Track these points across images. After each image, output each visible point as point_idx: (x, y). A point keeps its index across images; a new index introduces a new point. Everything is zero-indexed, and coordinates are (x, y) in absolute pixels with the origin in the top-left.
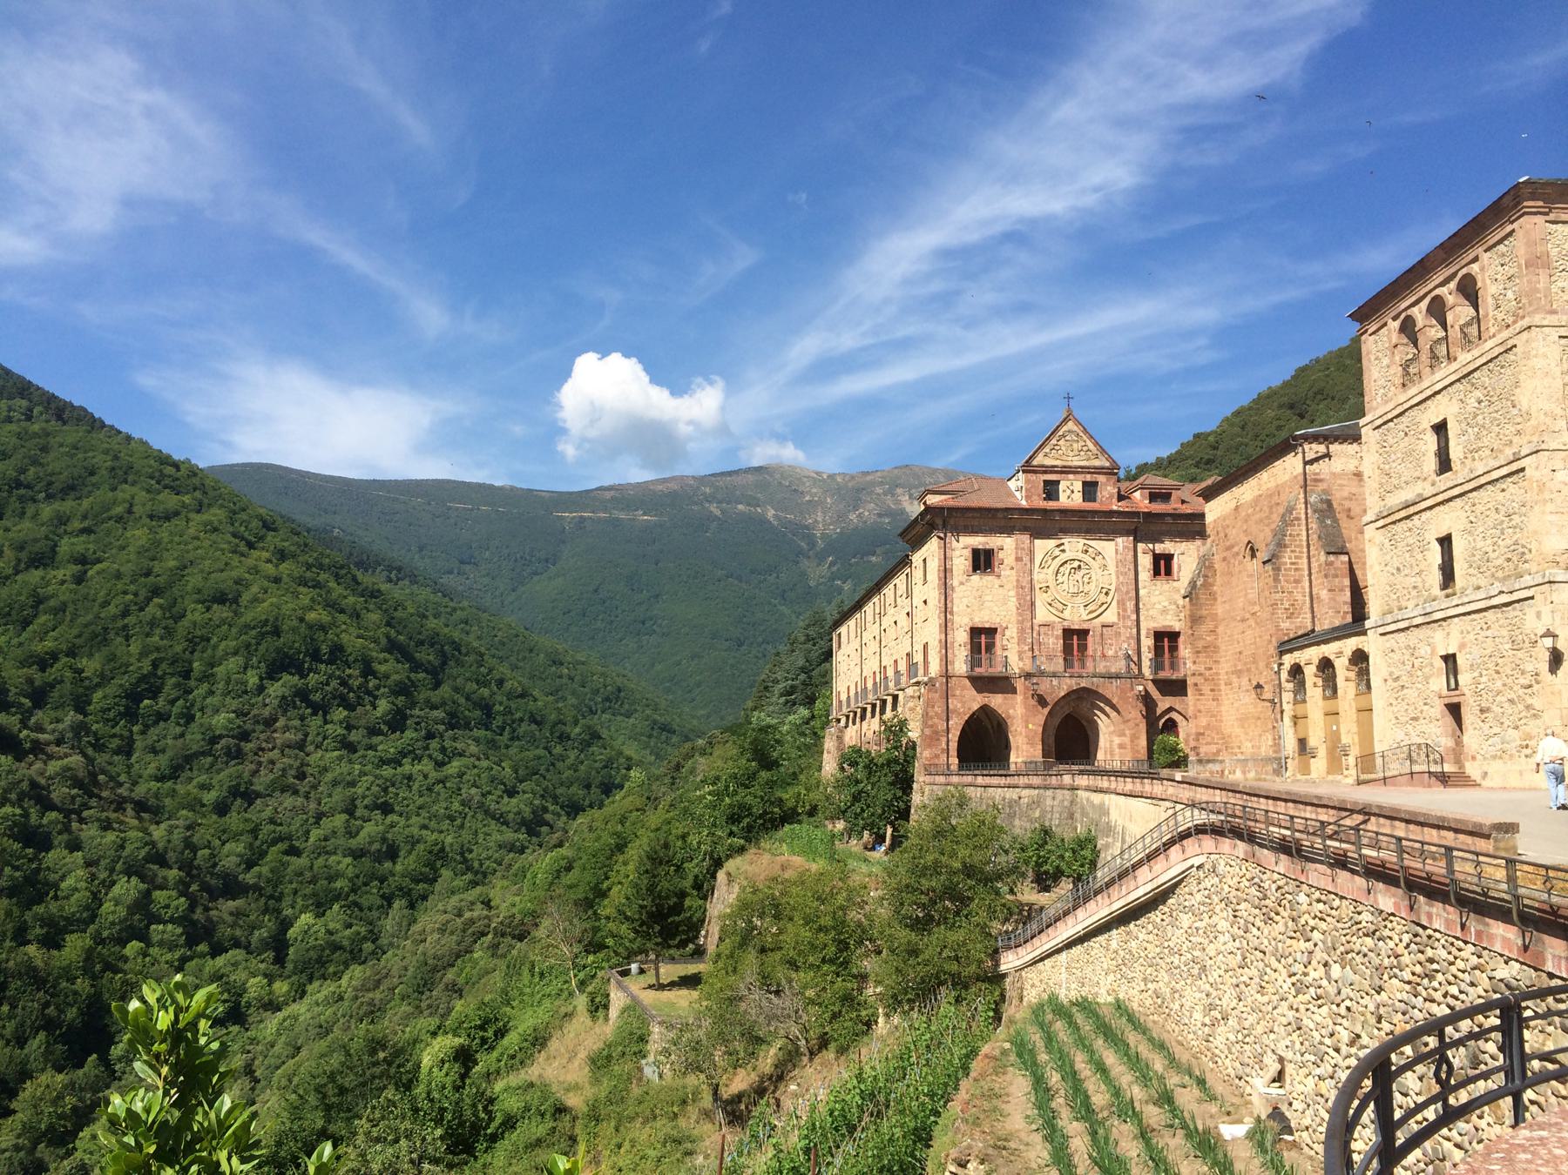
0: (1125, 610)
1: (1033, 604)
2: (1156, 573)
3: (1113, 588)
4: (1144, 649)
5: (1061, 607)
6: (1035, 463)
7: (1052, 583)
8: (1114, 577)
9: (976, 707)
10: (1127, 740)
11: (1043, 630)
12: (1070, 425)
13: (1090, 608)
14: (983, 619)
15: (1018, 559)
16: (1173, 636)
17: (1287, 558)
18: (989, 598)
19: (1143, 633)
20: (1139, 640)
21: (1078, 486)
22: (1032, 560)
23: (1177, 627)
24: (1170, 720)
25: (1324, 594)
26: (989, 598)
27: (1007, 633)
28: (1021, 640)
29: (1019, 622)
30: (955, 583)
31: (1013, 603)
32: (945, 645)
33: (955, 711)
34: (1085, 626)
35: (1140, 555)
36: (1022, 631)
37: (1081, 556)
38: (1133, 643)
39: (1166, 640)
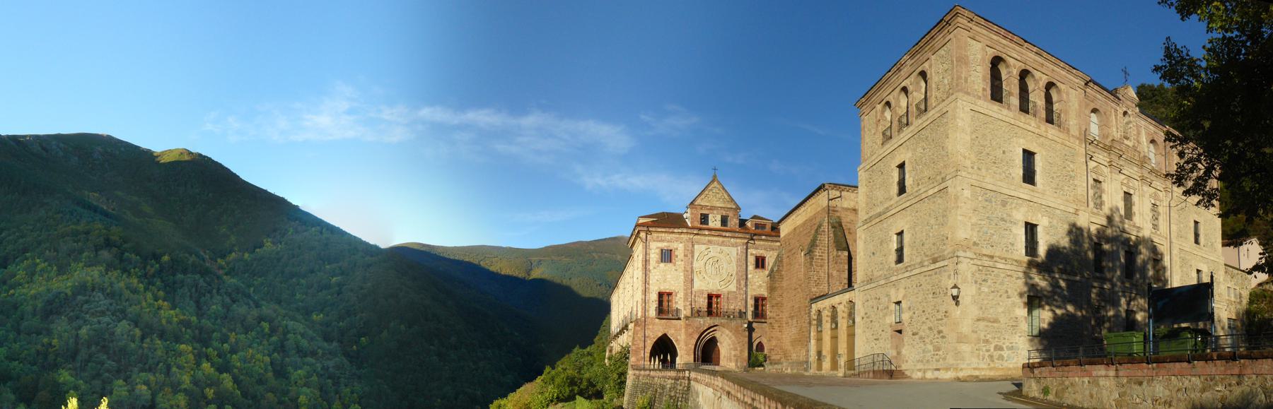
2: (757, 266)
14: (665, 288)
16: (764, 299)
17: (817, 253)
21: (719, 218)
23: (766, 294)
25: (835, 273)
28: (686, 299)
32: (645, 301)
36: (686, 295)
39: (759, 301)
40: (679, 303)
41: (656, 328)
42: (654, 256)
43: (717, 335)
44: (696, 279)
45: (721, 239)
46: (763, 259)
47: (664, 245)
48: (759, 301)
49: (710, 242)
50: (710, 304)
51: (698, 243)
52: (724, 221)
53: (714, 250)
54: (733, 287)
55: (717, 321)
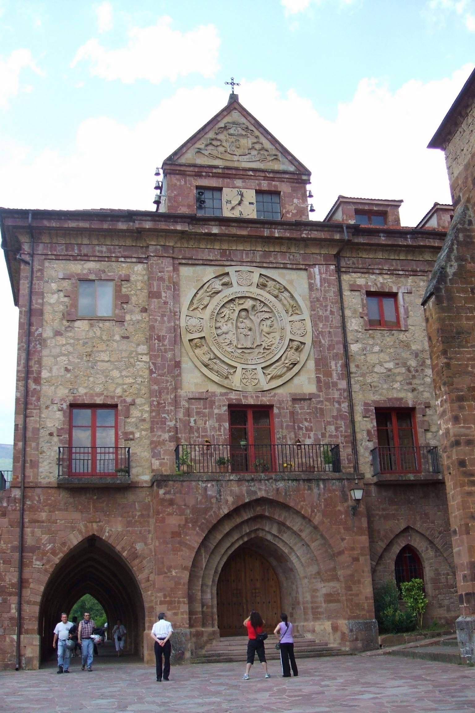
0: (329, 374)
3: (308, 340)
4: (361, 436)
5: (224, 369)
6: (183, 160)
8: (308, 324)
9: (75, 539)
11: (195, 407)
13: (272, 371)
15: (153, 295)
18: (105, 357)
19: (359, 409)
20: (353, 422)
24: (408, 549)
26: (105, 357)
27: (135, 413)
29: (152, 393)
30: (48, 333)
31: (143, 363)
33: (34, 549)
34: (265, 400)
35: (346, 293)
36: (158, 408)
37: (255, 291)
39: (394, 419)
54: (306, 383)
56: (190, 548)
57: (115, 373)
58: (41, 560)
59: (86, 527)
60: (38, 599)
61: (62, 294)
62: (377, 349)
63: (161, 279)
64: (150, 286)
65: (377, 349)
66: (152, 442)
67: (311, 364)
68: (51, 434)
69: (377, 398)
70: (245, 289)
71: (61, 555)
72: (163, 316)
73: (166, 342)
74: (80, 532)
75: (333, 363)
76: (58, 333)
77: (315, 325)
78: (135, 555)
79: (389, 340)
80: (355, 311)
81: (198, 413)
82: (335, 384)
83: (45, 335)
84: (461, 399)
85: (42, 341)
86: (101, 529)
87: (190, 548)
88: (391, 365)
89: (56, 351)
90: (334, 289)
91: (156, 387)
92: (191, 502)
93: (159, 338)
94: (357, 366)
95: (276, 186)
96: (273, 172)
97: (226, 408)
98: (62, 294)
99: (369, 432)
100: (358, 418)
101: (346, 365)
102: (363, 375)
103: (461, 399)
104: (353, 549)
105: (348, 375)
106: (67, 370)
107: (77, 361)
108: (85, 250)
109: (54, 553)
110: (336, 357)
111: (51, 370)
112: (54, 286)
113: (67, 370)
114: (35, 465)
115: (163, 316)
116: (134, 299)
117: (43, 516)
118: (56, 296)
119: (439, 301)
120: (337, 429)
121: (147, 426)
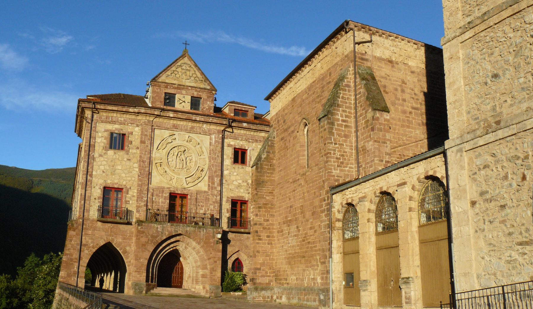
0: (213, 183)
1: (150, 174)
2: (236, 161)
3: (206, 167)
4: (224, 211)
6: (160, 80)
7: (164, 161)
8: (207, 160)
9: (102, 243)
10: (207, 272)
12: (186, 60)
14: (112, 181)
15: (142, 142)
16: (244, 202)
17: (339, 116)
19: (224, 199)
21: (188, 99)
22: (152, 144)
23: (247, 197)
25: (370, 145)
27: (130, 193)
28: (139, 198)
29: (139, 185)
30: (96, 155)
33: (85, 245)
34: (185, 192)
36: (140, 192)
38: (217, 205)
39: (237, 205)
40: (131, 202)
41: (97, 234)
42: (101, 140)
43: (181, 247)
44: (154, 173)
45: (190, 124)
46: (244, 152)
47: (115, 127)
48: (237, 205)
49: (175, 127)
50: (172, 207)
51: (160, 128)
52: (195, 102)
53: (181, 138)
54: (203, 186)
55: (180, 228)
56: (149, 251)
57: (123, 175)
58: (88, 250)
59: (107, 238)
60: (86, 265)
61: (103, 138)
62: (235, 174)
63: (146, 135)
64: (141, 138)
65: (235, 174)
66: (137, 206)
67: (206, 178)
68: (95, 199)
69: (232, 195)
70: (182, 142)
71: (96, 249)
72: (146, 152)
73: (146, 164)
74: (105, 240)
75: (216, 179)
76: (101, 156)
77: (210, 161)
78: (125, 252)
79: (241, 170)
80: (228, 156)
81: (157, 195)
82: (215, 188)
83: (95, 156)
84: (260, 207)
85: (94, 159)
86: (113, 240)
87: (149, 251)
88: (240, 181)
89: (99, 163)
90: (220, 146)
91: (140, 183)
92: (151, 233)
93: (143, 162)
94: (226, 181)
95: (200, 95)
96: (200, 88)
97: (168, 194)
98: (103, 138)
99: (227, 210)
100: (224, 203)
101: (221, 181)
102: (228, 185)
103: (260, 207)
104: (215, 258)
105: (221, 184)
106: (103, 172)
107: (108, 168)
108: (114, 119)
109: (93, 247)
110: (217, 176)
111: (96, 172)
112: (100, 134)
113: (103, 172)
114: (88, 211)
115: (146, 152)
116: (133, 143)
117: (90, 232)
118: (100, 139)
119: (257, 168)
120: (214, 207)
121: (136, 198)
